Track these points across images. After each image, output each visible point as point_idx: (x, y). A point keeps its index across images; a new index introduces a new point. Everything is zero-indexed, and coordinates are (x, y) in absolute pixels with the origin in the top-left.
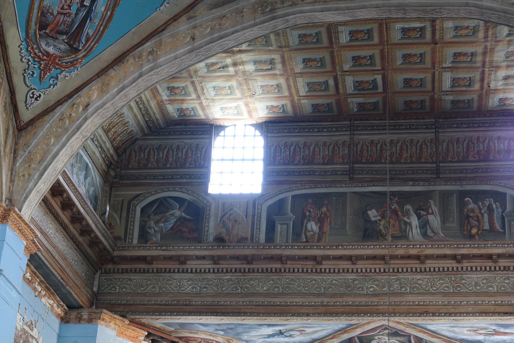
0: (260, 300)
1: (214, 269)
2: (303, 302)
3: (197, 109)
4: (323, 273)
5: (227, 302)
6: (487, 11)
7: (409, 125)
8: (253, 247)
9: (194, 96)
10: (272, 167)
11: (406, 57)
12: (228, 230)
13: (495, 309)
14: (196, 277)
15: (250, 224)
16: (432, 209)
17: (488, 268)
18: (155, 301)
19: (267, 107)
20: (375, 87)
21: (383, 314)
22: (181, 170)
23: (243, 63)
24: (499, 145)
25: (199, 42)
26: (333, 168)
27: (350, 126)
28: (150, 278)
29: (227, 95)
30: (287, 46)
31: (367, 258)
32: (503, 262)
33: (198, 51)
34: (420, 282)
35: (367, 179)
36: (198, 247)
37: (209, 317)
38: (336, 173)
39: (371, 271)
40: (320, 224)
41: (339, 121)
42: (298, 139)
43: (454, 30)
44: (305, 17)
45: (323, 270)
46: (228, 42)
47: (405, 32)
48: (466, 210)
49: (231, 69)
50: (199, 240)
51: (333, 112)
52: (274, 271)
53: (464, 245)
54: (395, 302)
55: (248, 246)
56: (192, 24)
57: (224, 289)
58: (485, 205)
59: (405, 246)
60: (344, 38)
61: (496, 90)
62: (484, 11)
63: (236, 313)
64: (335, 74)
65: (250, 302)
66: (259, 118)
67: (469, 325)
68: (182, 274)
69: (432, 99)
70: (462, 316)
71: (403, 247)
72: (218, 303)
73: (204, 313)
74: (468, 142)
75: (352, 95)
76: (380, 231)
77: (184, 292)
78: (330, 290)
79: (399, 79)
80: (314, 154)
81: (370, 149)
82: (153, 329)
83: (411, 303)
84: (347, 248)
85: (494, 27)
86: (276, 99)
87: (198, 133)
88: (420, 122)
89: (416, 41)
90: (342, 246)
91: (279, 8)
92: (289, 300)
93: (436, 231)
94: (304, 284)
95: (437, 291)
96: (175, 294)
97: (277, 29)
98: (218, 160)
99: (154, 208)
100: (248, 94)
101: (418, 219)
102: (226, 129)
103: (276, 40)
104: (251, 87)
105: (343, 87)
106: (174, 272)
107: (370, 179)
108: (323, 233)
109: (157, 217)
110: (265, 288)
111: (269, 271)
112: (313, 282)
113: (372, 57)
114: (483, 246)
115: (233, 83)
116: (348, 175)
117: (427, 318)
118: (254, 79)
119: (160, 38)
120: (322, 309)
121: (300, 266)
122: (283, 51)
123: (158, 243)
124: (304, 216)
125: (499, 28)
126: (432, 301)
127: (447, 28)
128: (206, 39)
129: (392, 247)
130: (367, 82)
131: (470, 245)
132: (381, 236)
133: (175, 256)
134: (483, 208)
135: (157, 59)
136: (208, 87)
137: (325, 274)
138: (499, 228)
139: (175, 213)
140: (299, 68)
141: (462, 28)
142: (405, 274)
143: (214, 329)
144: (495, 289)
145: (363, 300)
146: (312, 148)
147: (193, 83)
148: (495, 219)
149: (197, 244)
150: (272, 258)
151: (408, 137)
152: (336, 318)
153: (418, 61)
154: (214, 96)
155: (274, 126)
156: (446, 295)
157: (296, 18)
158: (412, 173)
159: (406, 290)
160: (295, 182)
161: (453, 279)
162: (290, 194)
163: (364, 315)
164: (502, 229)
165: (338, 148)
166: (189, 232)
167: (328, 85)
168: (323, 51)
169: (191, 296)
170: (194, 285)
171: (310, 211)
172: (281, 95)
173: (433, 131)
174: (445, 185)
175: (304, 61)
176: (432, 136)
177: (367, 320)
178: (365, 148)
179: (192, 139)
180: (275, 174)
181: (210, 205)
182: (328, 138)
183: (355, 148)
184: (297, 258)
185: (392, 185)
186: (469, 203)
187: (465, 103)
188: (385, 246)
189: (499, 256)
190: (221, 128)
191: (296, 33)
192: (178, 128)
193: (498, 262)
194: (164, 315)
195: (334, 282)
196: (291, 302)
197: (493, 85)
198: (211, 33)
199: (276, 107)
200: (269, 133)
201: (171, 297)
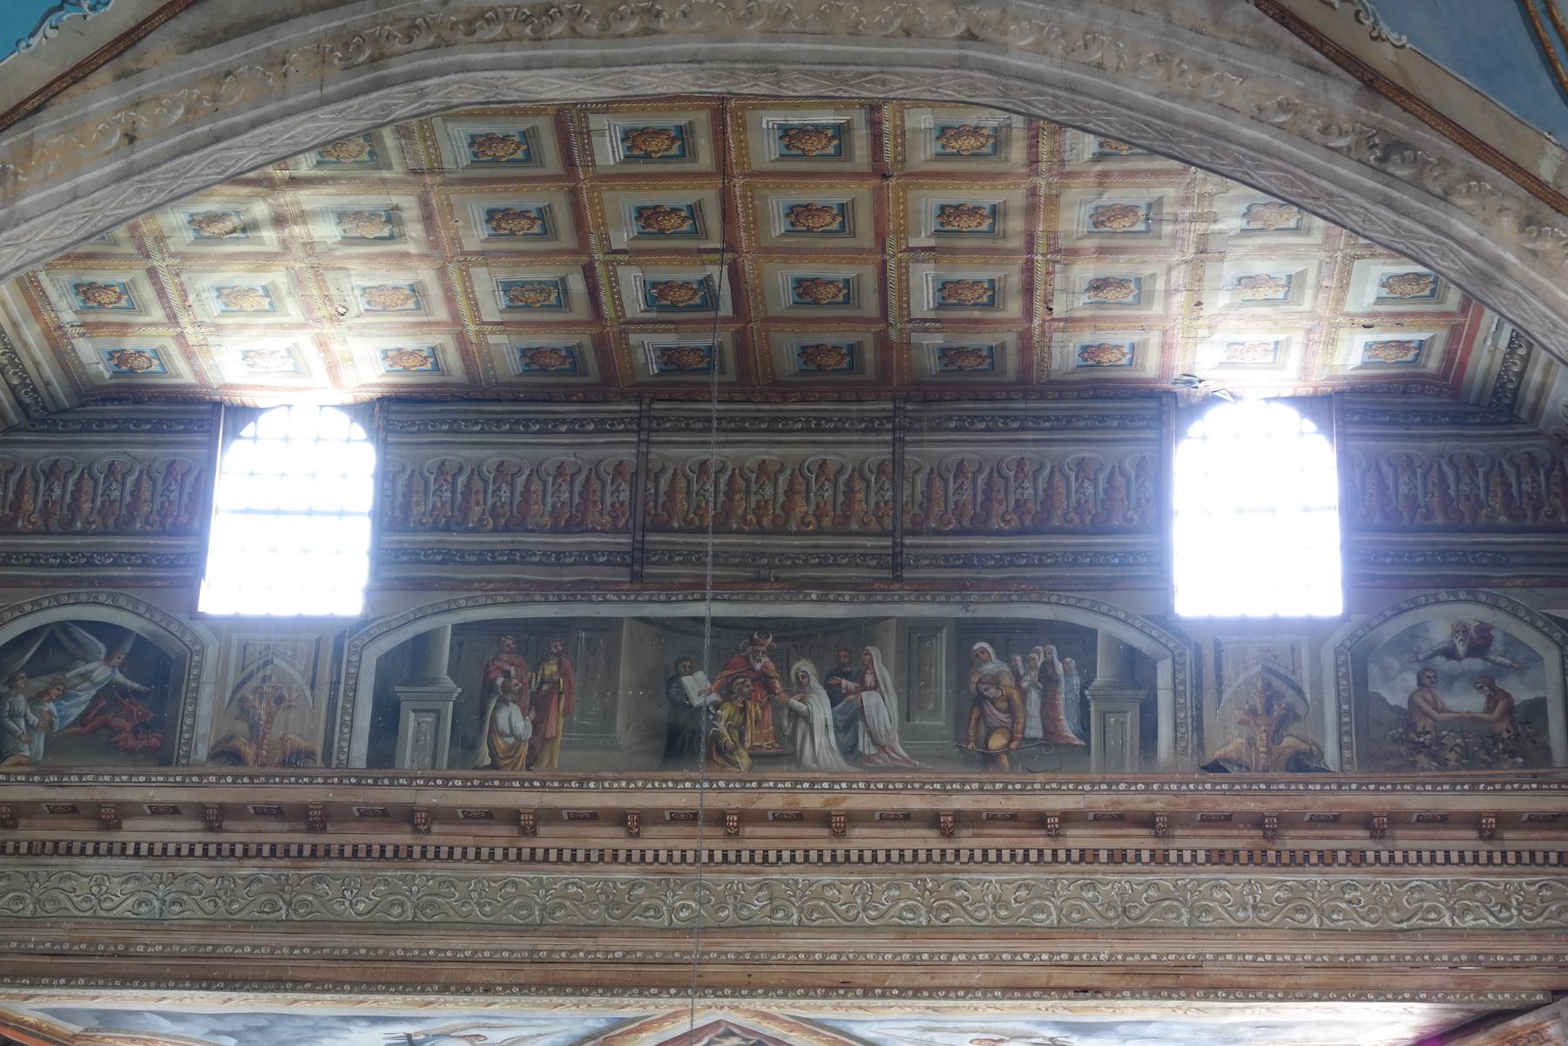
0: (345, 941)
1: (206, 844)
2: (476, 951)
3: (168, 355)
4: (539, 862)
5: (242, 947)
6: (1020, 83)
7: (815, 419)
8: (326, 778)
9: (158, 314)
10: (396, 538)
11: (797, 213)
12: (253, 727)
13: (1050, 976)
14: (149, 871)
15: (324, 709)
16: (874, 673)
17: (1033, 855)
18: (20, 942)
19: (385, 352)
20: (711, 301)
21: (716, 988)
22: (119, 540)
23: (303, 217)
24: (1081, 485)
25: (150, 150)
26: (584, 543)
27: (640, 418)
28: (9, 870)
29: (260, 312)
30: (436, 169)
31: (672, 819)
32: (1078, 839)
33: (144, 176)
34: (829, 893)
35: (682, 580)
36: (156, 776)
37: (186, 993)
38: (591, 558)
39: (683, 858)
40: (536, 711)
41: (606, 401)
42: (479, 453)
43: (938, 138)
44: (475, 84)
45: (540, 854)
46: (243, 152)
47: (791, 138)
48: (975, 679)
49: (269, 236)
50: (163, 757)
51: (585, 374)
52: (389, 854)
53: (963, 784)
54: (754, 953)
55: (312, 778)
56: (130, 93)
57: (235, 907)
58: (1032, 663)
59: (788, 785)
60: (608, 151)
61: (1071, 321)
62: (1012, 82)
63: (271, 980)
64: (585, 259)
65: (313, 949)
66: (363, 386)
67: (977, 1025)
68: (108, 860)
69: (883, 342)
70: (951, 998)
71: (780, 785)
72: (213, 951)
73: (170, 979)
74: (990, 475)
75: (643, 324)
76: (717, 736)
77: (111, 914)
78: (558, 914)
79: (779, 279)
80: (525, 500)
81: (695, 487)
82: (16, 1029)
83: (802, 956)
84: (611, 788)
85: (1053, 134)
86: (411, 331)
87: (176, 427)
88: (848, 411)
89: (826, 166)
90: (597, 780)
91: (399, 55)
92: (432, 943)
93: (883, 741)
94: (480, 894)
95: (880, 922)
96: (83, 920)
97: (392, 117)
98: (234, 512)
99: (30, 654)
100: (323, 313)
101: (833, 704)
102: (262, 418)
103: (402, 150)
104: (333, 291)
105: (614, 300)
106: (82, 852)
107: (692, 580)
108: (545, 740)
109: (38, 684)
110: (361, 907)
111: (376, 853)
112: (509, 889)
113: (695, 211)
114: (1018, 786)
115: (278, 277)
116: (627, 565)
117: (847, 1002)
118: (341, 268)
119: (28, 133)
120: (531, 972)
121: (469, 840)
122: (425, 185)
123: (36, 763)
124: (488, 689)
125: (1068, 134)
126: (863, 950)
127: (916, 131)
128: (172, 141)
129: (748, 785)
130: (685, 285)
131: (982, 783)
132: (720, 752)
133: (86, 804)
134: (1026, 674)
135: (13, 200)
136: (199, 286)
137: (546, 866)
138: (1072, 735)
139: (92, 671)
140: (476, 236)
141: (959, 132)
142: (786, 868)
143: (206, 1030)
144: (1054, 916)
145: (657, 945)
146: (521, 480)
147: (152, 273)
148: (1062, 708)
149: (156, 769)
150: (384, 816)
151: (812, 455)
152: (574, 999)
153: (835, 226)
154: (219, 316)
155: (409, 412)
156: (907, 933)
157: (447, 86)
158: (819, 565)
159: (789, 916)
160: (466, 585)
161: (930, 885)
162: (449, 621)
163: (660, 992)
164: (1079, 736)
165: (599, 484)
166: (135, 731)
167: (566, 290)
168: (548, 189)
169: (133, 927)
170: (143, 895)
171: (507, 674)
172: (425, 319)
173: (888, 437)
174: (917, 601)
175: (491, 215)
176: (885, 453)
177: (670, 1006)
178: (682, 484)
179: (155, 444)
180: (406, 558)
181: (203, 649)
182: (572, 451)
183: (651, 485)
184: (461, 816)
185: (758, 597)
186: (985, 656)
187: (980, 356)
188: (727, 785)
189: (1067, 818)
190: (245, 413)
191: (461, 132)
192: (108, 411)
193: (1064, 836)
194: (46, 986)
195: (572, 889)
196: (439, 950)
197: (1059, 309)
198: (186, 124)
199: (413, 353)
200: (391, 432)
201: (70, 930)
